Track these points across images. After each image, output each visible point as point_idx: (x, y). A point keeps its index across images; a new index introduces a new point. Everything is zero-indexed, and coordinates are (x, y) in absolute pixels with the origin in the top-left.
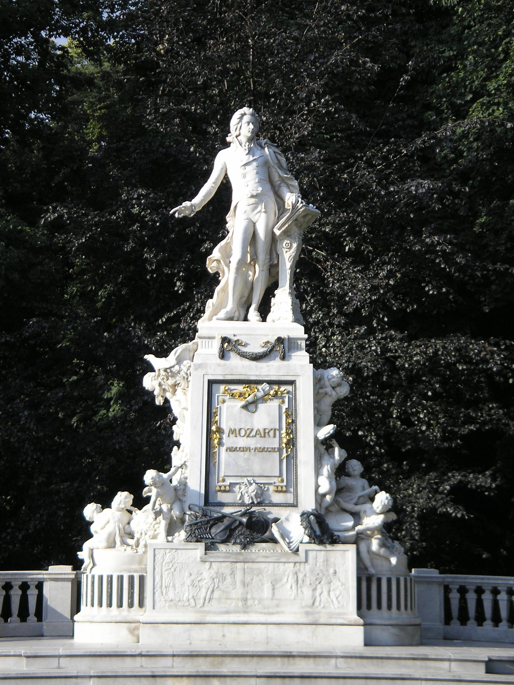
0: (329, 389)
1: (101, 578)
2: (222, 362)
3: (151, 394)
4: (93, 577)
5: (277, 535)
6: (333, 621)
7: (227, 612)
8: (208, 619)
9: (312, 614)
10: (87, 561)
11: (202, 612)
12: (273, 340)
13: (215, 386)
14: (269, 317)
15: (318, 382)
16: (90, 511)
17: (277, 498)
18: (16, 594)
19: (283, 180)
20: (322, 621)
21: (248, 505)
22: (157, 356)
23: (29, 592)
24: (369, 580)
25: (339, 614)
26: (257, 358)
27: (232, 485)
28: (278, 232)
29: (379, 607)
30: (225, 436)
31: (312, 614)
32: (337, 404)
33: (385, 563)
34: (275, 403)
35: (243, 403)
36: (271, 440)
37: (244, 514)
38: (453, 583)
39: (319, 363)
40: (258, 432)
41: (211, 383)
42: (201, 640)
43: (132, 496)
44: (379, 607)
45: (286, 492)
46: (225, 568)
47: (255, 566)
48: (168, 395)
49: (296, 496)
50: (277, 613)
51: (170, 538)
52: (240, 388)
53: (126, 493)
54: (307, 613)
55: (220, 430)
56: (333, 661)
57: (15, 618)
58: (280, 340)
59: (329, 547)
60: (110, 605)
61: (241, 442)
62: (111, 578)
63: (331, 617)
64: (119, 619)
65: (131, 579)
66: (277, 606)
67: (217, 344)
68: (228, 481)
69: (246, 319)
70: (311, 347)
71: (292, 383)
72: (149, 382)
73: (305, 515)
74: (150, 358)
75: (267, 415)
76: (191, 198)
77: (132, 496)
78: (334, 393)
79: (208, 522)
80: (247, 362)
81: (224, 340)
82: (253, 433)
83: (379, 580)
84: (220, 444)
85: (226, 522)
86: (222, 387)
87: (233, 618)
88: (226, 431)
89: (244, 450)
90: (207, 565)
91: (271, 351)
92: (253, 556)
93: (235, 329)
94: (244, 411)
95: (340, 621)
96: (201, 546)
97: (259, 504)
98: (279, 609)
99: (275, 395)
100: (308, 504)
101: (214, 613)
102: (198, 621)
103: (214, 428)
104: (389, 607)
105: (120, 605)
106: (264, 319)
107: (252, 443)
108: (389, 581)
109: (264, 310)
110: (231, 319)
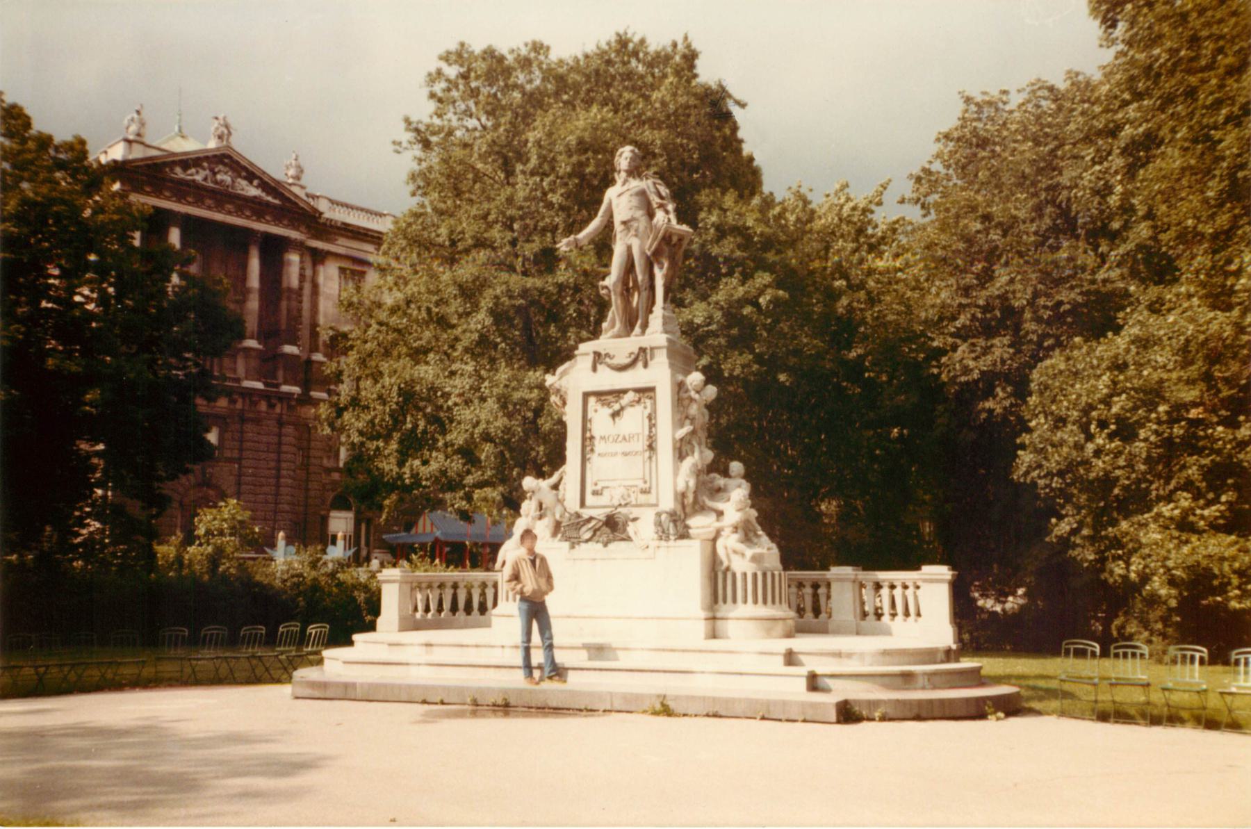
5: (631, 533)
12: (636, 351)
14: (648, 331)
15: (680, 387)
26: (622, 368)
27: (603, 488)
30: (596, 442)
34: (639, 408)
35: (610, 411)
38: (884, 581)
40: (624, 438)
41: (586, 395)
44: (734, 601)
49: (657, 499)
55: (592, 438)
58: (643, 350)
67: (590, 358)
71: (652, 389)
73: (659, 515)
75: (634, 419)
76: (580, 230)
78: (697, 396)
84: (592, 450)
85: (593, 523)
97: (626, 505)
99: (639, 401)
100: (668, 503)
103: (588, 435)
106: (643, 333)
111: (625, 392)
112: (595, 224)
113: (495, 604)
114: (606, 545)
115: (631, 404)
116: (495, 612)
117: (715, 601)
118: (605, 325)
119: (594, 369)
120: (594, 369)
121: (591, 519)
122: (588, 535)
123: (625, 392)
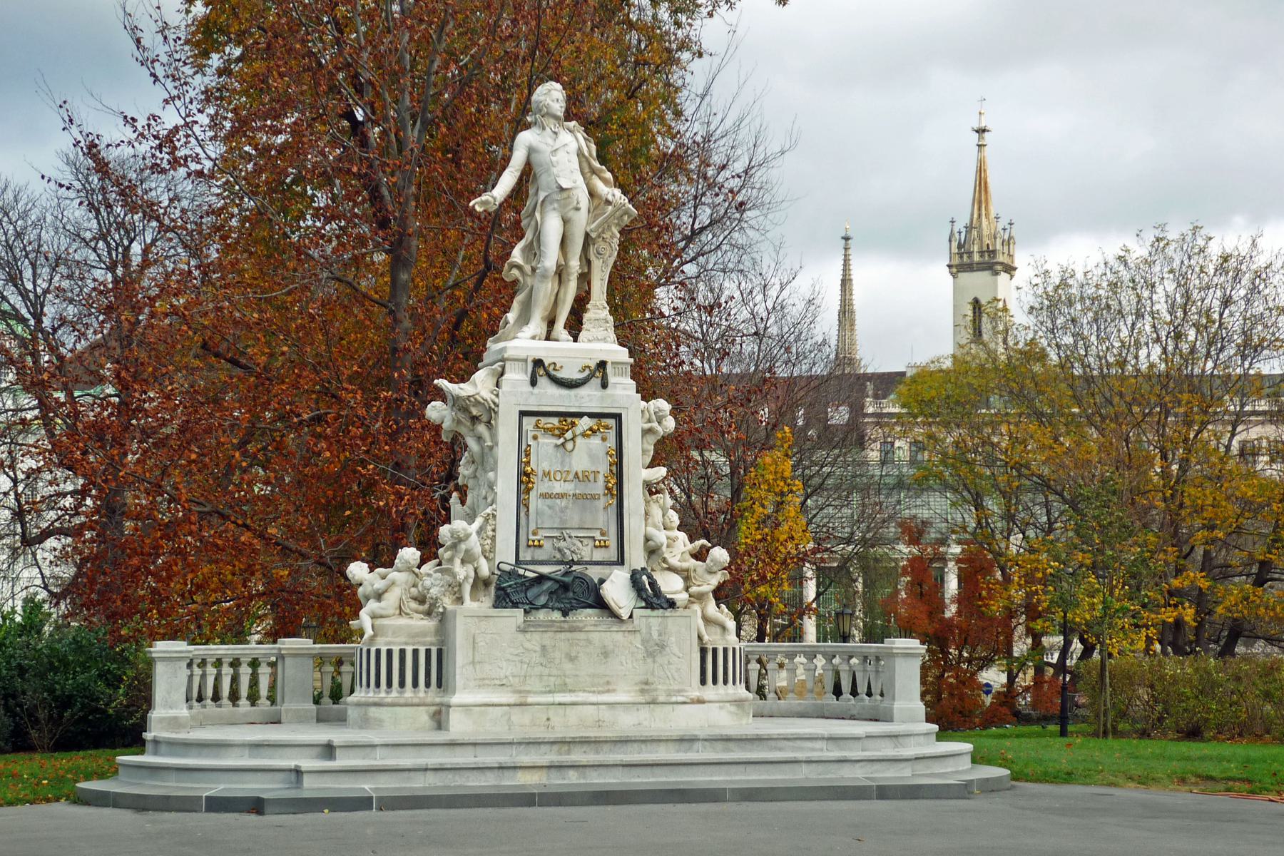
0: (655, 425)
1: (390, 652)
2: (536, 390)
3: (437, 428)
4: (378, 651)
6: (674, 699)
7: (550, 692)
8: (530, 700)
9: (647, 691)
10: (369, 632)
11: (520, 692)
12: (593, 365)
13: (525, 420)
14: (582, 335)
16: (357, 570)
17: (599, 555)
18: (245, 671)
19: (594, 171)
20: (661, 699)
21: (566, 563)
22: (451, 381)
23: (260, 670)
24: (703, 651)
25: (679, 691)
28: (593, 235)
29: (715, 682)
31: (647, 691)
32: (661, 443)
33: (718, 630)
34: (596, 441)
35: (562, 440)
36: (591, 485)
37: (566, 574)
39: (647, 393)
42: (524, 724)
43: (419, 553)
44: (715, 682)
45: (606, 547)
46: (548, 639)
47: (582, 636)
48: (463, 430)
50: (608, 691)
51: (475, 605)
52: (555, 421)
53: (413, 550)
54: (642, 691)
56: (699, 745)
57: (244, 702)
58: (602, 365)
59: (668, 612)
60: (402, 684)
61: (558, 487)
62: (402, 652)
63: (669, 695)
64: (416, 701)
65: (428, 652)
66: (608, 683)
68: (542, 534)
69: (548, 338)
70: (637, 373)
71: (618, 417)
72: (435, 411)
74: (442, 383)
75: (589, 453)
77: (419, 553)
79: (523, 584)
80: (564, 392)
81: (538, 363)
82: (571, 476)
83: (715, 651)
86: (534, 419)
87: (559, 698)
88: (540, 474)
89: (561, 496)
90: (528, 635)
91: (592, 375)
92: (581, 625)
93: (543, 350)
94: (561, 449)
95: (680, 699)
96: (519, 613)
97: (579, 563)
98: (610, 688)
101: (535, 693)
102: (518, 702)
104: (725, 682)
105: (415, 684)
106: (575, 340)
107: (569, 488)
108: (725, 650)
109: (575, 326)
110: (533, 338)
111: (580, 415)
112: (507, 181)
113: (352, 691)
114: (565, 614)
115: (584, 435)
116: (350, 699)
117: (703, 682)
118: (511, 316)
119: (533, 383)
120: (533, 383)
121: (541, 578)
122: (543, 600)
123: (580, 415)
